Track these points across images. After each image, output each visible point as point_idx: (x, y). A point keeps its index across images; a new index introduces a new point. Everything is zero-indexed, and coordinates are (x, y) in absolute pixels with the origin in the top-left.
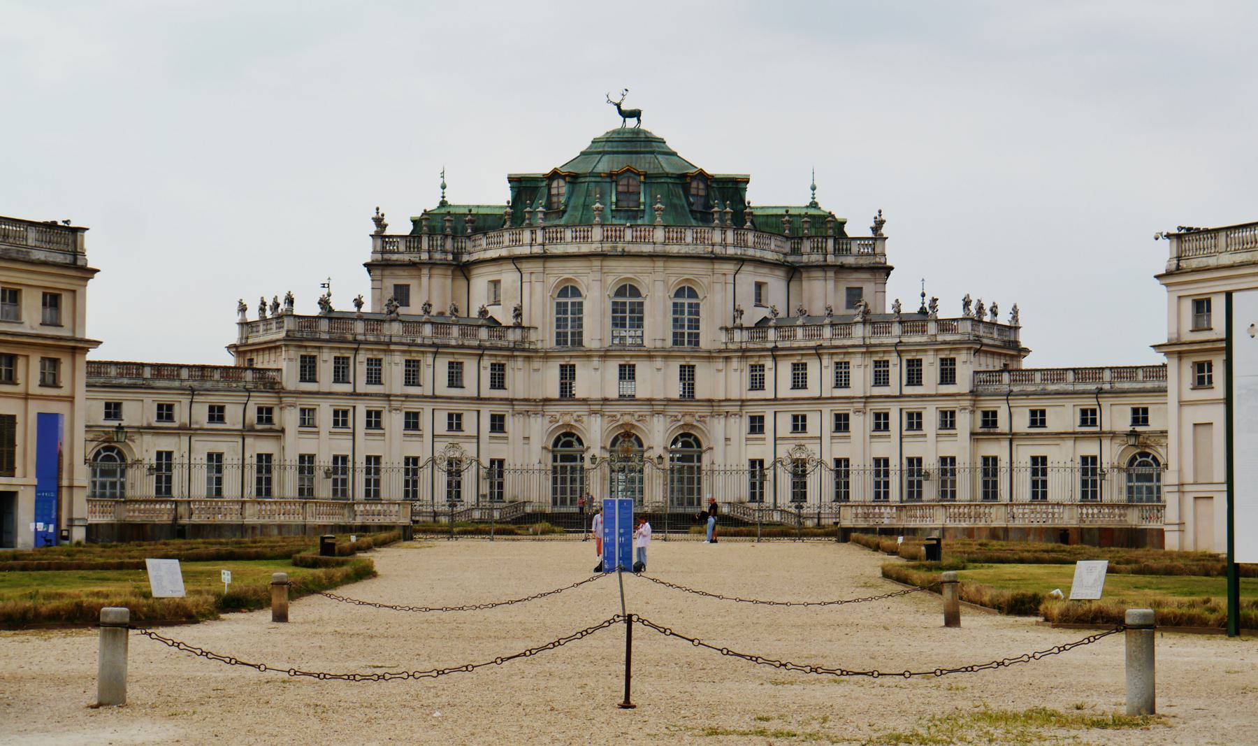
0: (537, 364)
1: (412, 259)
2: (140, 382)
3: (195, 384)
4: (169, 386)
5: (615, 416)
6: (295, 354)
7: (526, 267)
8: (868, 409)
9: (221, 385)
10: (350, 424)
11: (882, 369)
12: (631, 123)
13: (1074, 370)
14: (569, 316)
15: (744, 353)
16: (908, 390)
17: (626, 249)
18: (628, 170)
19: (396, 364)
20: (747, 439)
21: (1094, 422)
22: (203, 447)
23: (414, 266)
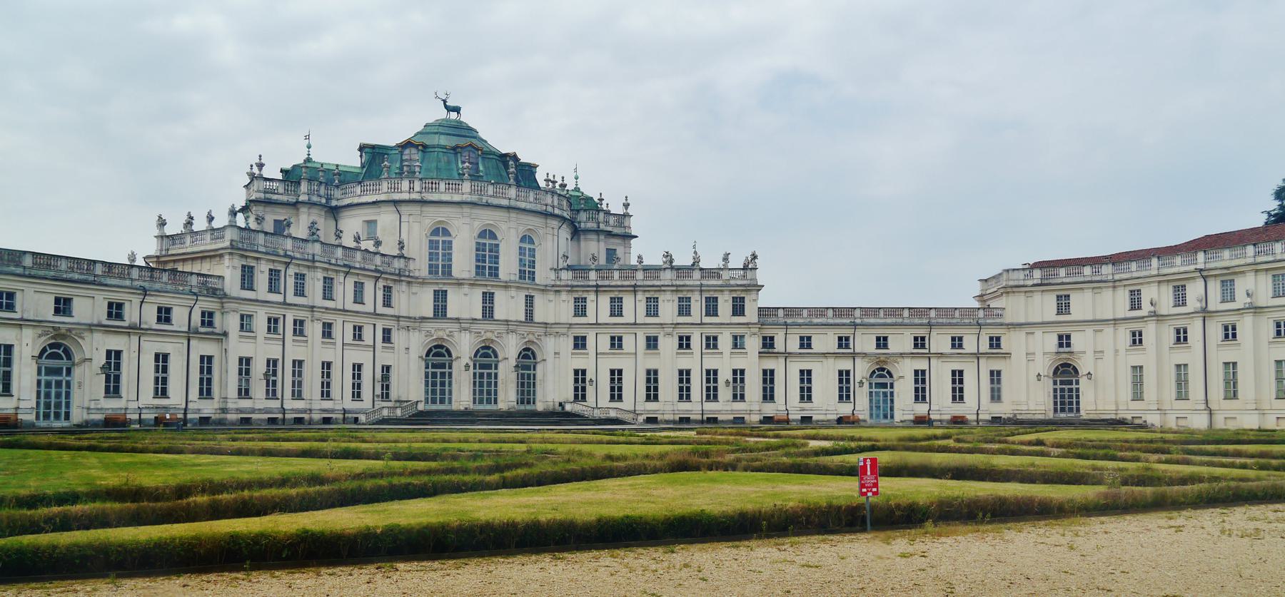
0: (415, 289)
1: (290, 200)
2: (91, 278)
3: (146, 285)
4: (120, 284)
5: (480, 333)
6: (238, 262)
7: (403, 209)
8: (675, 333)
9: (169, 287)
10: (281, 330)
11: (684, 303)
12: (453, 115)
13: (833, 308)
14: (440, 251)
15: (571, 289)
16: (707, 320)
17: (489, 201)
18: (470, 145)
19: (318, 280)
20: (572, 354)
21: (847, 346)
22: (152, 347)
23: (295, 205)
